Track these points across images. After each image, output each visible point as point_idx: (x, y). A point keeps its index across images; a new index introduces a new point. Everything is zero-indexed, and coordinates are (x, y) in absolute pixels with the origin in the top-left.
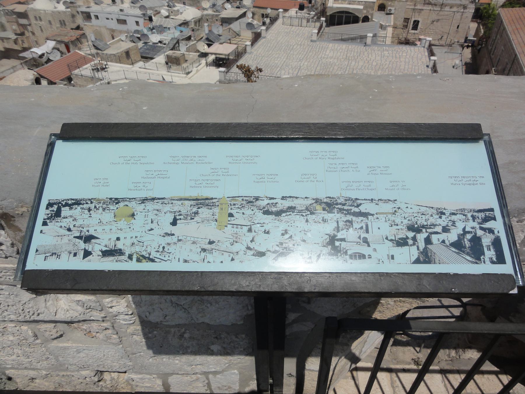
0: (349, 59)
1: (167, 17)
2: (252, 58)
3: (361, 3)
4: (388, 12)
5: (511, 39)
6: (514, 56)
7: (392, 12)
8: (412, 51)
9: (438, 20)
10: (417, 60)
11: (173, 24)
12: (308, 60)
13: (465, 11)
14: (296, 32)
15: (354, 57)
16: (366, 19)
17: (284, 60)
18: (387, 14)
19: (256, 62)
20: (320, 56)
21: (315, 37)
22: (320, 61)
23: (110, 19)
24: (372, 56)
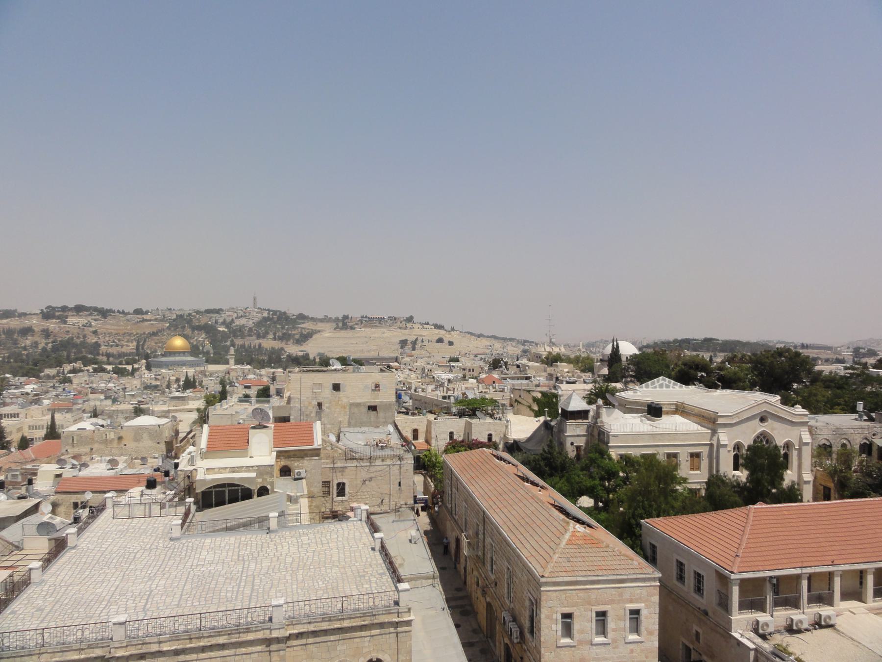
0: (243, 560)
3: (251, 468)
4: (296, 476)
6: (482, 513)
7: (302, 476)
9: (370, 479)
10: (356, 543)
13: (402, 463)
16: (263, 491)
18: (296, 479)
20: (189, 564)
21: (177, 532)
22: (190, 572)
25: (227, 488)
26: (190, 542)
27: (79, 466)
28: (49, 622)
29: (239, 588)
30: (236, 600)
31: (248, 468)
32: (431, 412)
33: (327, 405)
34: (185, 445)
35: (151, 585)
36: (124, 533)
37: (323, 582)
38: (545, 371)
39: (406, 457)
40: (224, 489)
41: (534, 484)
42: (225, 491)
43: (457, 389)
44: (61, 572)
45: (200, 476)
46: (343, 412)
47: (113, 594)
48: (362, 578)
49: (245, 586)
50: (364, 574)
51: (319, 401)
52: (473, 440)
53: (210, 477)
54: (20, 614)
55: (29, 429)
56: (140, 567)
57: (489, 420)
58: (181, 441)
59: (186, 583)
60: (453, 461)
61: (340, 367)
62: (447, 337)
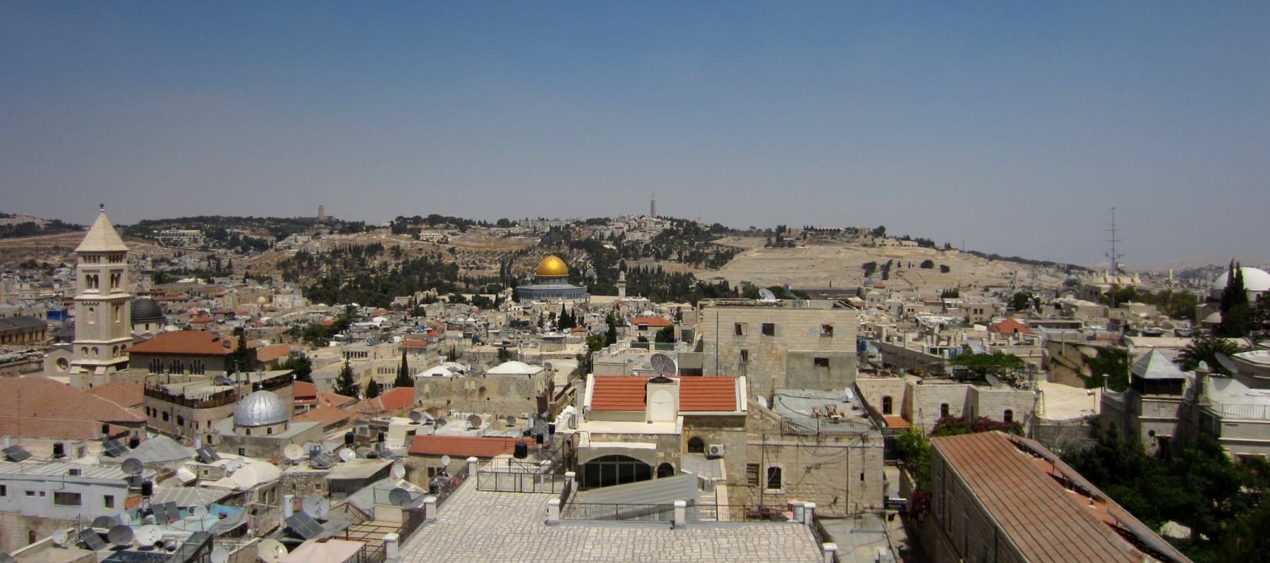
1: (192, 483)
3: (650, 437)
4: (711, 453)
5: (975, 494)
6: (993, 531)
7: (719, 453)
9: (818, 466)
11: (203, 500)
13: (866, 445)
14: (509, 506)
16: (666, 470)
18: (710, 458)
21: (554, 515)
23: (37, 493)
27: (434, 423)
31: (646, 437)
32: (911, 372)
33: (755, 355)
34: (561, 404)
38: (1106, 315)
39: (872, 436)
40: (614, 463)
41: (1080, 491)
42: (615, 465)
43: (955, 339)
44: (419, 550)
45: (583, 442)
52: (980, 418)
53: (595, 445)
55: (379, 372)
56: (509, 554)
57: (1006, 388)
58: (557, 398)
60: (946, 447)
61: (773, 300)
62: (939, 260)
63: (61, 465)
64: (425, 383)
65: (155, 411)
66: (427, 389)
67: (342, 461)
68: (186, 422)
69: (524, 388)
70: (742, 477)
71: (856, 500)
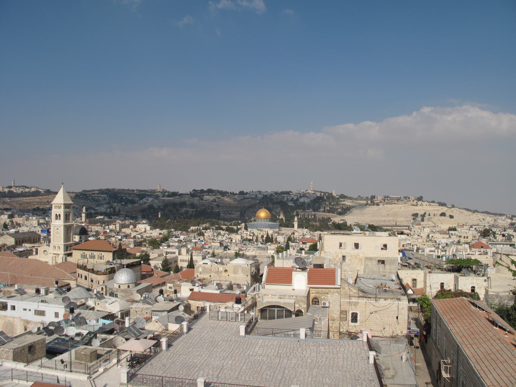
0: (280, 356)
2: (168, 357)
3: (292, 297)
4: (323, 305)
5: (449, 328)
8: (350, 345)
9: (376, 312)
10: (356, 356)
12: (233, 358)
14: (223, 327)
15: (286, 354)
17: (205, 358)
19: (171, 361)
20: (247, 353)
23: (28, 310)
24: (307, 353)
25: (277, 309)
26: (250, 340)
28: (167, 374)
29: (275, 373)
30: (272, 381)
35: (224, 362)
36: (214, 329)
37: (329, 379)
39: (402, 298)
40: (274, 309)
44: (178, 346)
46: (360, 264)
47: (202, 364)
48: (357, 381)
49: (278, 373)
50: (358, 378)
51: (344, 255)
52: (459, 290)
54: (155, 366)
56: (219, 350)
59: (243, 365)
60: (437, 305)
61: (359, 232)
63: (38, 297)
64: (199, 267)
65: (81, 275)
66: (200, 270)
67: (158, 302)
68: (94, 281)
69: (245, 270)
70: (337, 317)
71: (394, 330)
